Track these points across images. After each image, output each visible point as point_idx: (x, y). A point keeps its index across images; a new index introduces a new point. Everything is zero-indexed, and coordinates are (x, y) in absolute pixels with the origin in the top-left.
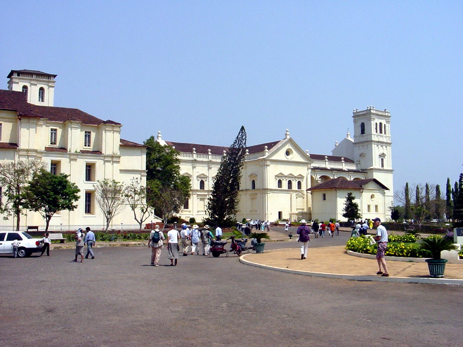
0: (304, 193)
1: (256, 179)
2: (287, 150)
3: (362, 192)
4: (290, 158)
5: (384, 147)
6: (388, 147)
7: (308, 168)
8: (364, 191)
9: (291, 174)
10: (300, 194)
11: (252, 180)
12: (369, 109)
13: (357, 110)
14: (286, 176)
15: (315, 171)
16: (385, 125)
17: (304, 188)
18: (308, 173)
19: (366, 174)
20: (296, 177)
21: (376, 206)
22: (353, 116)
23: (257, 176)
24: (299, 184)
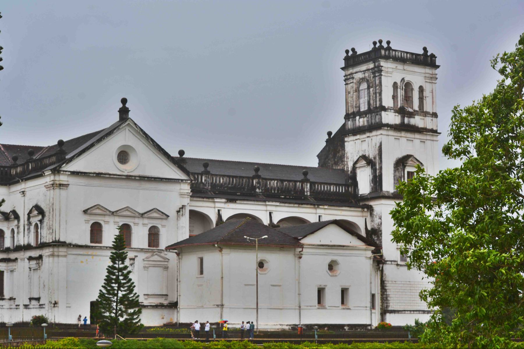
0: (167, 257)
2: (119, 151)
4: (127, 169)
5: (417, 142)
6: (428, 143)
7: (182, 195)
8: (305, 250)
9: (127, 209)
10: (156, 258)
11: (34, 224)
14: (113, 213)
15: (214, 202)
17: (164, 243)
18: (181, 206)
20: (142, 215)
21: (344, 292)
22: (343, 66)
23: (41, 212)
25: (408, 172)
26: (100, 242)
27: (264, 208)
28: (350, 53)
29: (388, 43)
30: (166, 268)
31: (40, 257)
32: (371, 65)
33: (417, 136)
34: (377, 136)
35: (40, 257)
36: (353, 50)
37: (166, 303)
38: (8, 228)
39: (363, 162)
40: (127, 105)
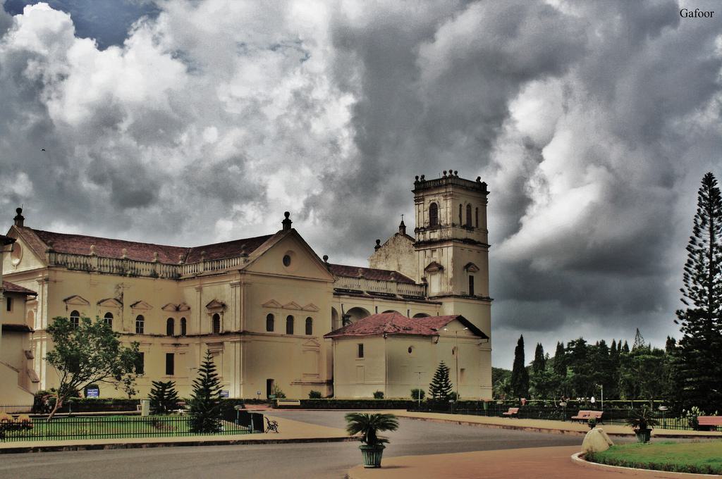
1: (222, 313)
3: (436, 343)
10: (311, 343)
11: (213, 314)
12: (448, 174)
13: (423, 177)
14: (282, 307)
16: (477, 209)
19: (438, 305)
24: (309, 322)
25: (470, 276)
26: (272, 330)
27: (371, 303)
28: (419, 180)
29: (456, 173)
30: (319, 352)
31: (222, 343)
32: (444, 191)
33: (475, 247)
34: (447, 247)
35: (222, 343)
36: (423, 177)
37: (318, 381)
38: (178, 318)
39: (436, 268)
40: (289, 218)
